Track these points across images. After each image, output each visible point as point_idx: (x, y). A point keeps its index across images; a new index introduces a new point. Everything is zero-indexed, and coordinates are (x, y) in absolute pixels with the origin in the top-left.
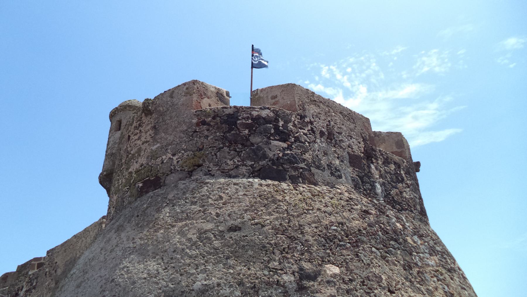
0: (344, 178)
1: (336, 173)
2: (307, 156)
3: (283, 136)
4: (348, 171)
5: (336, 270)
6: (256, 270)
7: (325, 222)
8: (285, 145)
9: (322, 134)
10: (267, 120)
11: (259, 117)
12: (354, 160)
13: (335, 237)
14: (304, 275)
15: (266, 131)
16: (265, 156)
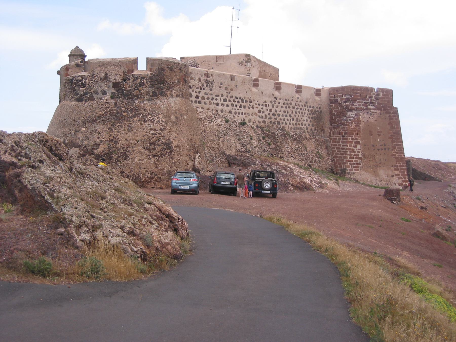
0: (108, 94)
1: (104, 93)
2: (92, 91)
3: (84, 85)
4: (112, 90)
7: (87, 115)
8: (84, 89)
9: (101, 79)
10: (80, 81)
11: (78, 80)
13: (88, 120)
14: (76, 131)
16: (78, 94)
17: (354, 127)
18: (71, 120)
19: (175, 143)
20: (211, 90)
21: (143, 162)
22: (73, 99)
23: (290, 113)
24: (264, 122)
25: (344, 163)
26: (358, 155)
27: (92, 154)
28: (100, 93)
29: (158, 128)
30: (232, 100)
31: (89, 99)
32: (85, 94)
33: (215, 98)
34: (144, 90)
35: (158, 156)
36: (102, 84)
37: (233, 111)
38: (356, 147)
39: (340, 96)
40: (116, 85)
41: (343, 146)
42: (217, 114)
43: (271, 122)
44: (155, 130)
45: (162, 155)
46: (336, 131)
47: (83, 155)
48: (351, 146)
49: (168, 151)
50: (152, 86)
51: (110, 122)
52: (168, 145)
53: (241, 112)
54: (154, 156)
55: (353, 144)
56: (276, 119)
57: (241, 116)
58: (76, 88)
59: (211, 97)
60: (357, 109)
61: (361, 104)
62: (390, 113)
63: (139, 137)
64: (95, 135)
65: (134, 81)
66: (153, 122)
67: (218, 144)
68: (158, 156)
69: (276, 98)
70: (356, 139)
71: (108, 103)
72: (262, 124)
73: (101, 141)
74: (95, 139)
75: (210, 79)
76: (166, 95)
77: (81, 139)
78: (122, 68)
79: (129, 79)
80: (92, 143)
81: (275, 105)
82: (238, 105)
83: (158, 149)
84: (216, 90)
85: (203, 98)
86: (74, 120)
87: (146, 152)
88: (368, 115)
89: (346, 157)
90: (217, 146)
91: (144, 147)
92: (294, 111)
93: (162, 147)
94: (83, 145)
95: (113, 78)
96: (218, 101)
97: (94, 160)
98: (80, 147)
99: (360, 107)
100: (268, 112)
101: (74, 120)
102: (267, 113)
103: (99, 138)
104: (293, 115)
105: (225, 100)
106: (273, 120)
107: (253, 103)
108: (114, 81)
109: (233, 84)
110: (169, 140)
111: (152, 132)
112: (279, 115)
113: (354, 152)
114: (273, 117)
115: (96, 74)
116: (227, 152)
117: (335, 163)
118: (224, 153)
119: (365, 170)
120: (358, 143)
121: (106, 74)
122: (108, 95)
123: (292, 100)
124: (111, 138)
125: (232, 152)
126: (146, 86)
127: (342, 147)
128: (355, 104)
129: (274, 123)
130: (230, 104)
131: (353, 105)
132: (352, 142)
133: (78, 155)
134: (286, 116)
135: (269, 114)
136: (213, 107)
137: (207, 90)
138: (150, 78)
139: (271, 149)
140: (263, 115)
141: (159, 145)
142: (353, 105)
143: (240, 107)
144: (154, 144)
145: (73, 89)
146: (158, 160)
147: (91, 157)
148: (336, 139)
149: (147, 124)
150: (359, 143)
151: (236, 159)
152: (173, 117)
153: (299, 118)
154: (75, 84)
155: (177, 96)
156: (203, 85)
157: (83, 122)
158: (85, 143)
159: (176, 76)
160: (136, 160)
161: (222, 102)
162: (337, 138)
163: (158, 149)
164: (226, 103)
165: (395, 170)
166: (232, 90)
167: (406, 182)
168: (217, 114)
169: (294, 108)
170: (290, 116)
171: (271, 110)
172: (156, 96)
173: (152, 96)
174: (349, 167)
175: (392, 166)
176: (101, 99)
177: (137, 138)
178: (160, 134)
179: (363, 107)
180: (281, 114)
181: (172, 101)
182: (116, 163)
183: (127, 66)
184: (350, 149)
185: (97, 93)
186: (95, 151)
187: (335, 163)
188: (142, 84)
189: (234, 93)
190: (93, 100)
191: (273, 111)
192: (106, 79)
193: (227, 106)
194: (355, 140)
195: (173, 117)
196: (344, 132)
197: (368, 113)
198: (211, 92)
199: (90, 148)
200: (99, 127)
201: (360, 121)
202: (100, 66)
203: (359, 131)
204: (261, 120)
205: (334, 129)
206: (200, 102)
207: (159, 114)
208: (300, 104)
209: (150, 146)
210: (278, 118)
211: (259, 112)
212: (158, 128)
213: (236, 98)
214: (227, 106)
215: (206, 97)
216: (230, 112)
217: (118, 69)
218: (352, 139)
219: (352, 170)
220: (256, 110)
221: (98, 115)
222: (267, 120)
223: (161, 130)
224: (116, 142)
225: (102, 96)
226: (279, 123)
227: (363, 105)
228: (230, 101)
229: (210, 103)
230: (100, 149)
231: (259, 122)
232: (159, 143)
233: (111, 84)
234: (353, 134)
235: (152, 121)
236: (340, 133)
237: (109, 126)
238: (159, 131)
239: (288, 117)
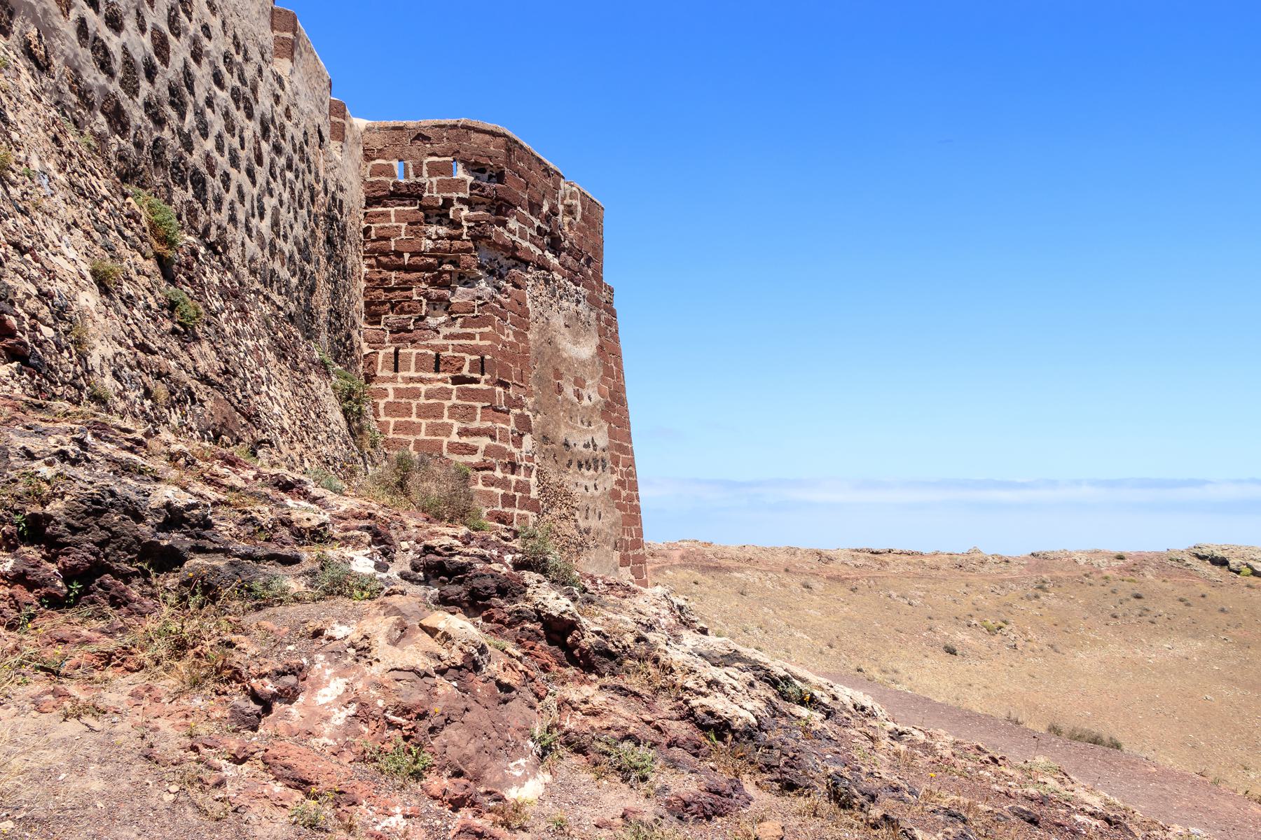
17: (511, 338)
26: (524, 487)
38: (518, 442)
39: (434, 170)
41: (463, 432)
46: (409, 351)
61: (529, 231)
70: (518, 403)
99: (526, 244)
113: (513, 467)
120: (524, 425)
123: (260, 71)
127: (455, 438)
128: (513, 224)
131: (504, 224)
134: (234, 162)
135: (151, 73)
139: (204, 379)
140: (114, 43)
142: (504, 224)
148: (416, 394)
153: (286, 216)
162: (423, 388)
170: (251, 173)
175: (615, 547)
179: (533, 248)
180: (217, 123)
191: (170, 73)
194: (515, 406)
196: (468, 358)
197: (547, 282)
201: (526, 313)
226: (199, 183)
227: (532, 240)
234: (506, 371)
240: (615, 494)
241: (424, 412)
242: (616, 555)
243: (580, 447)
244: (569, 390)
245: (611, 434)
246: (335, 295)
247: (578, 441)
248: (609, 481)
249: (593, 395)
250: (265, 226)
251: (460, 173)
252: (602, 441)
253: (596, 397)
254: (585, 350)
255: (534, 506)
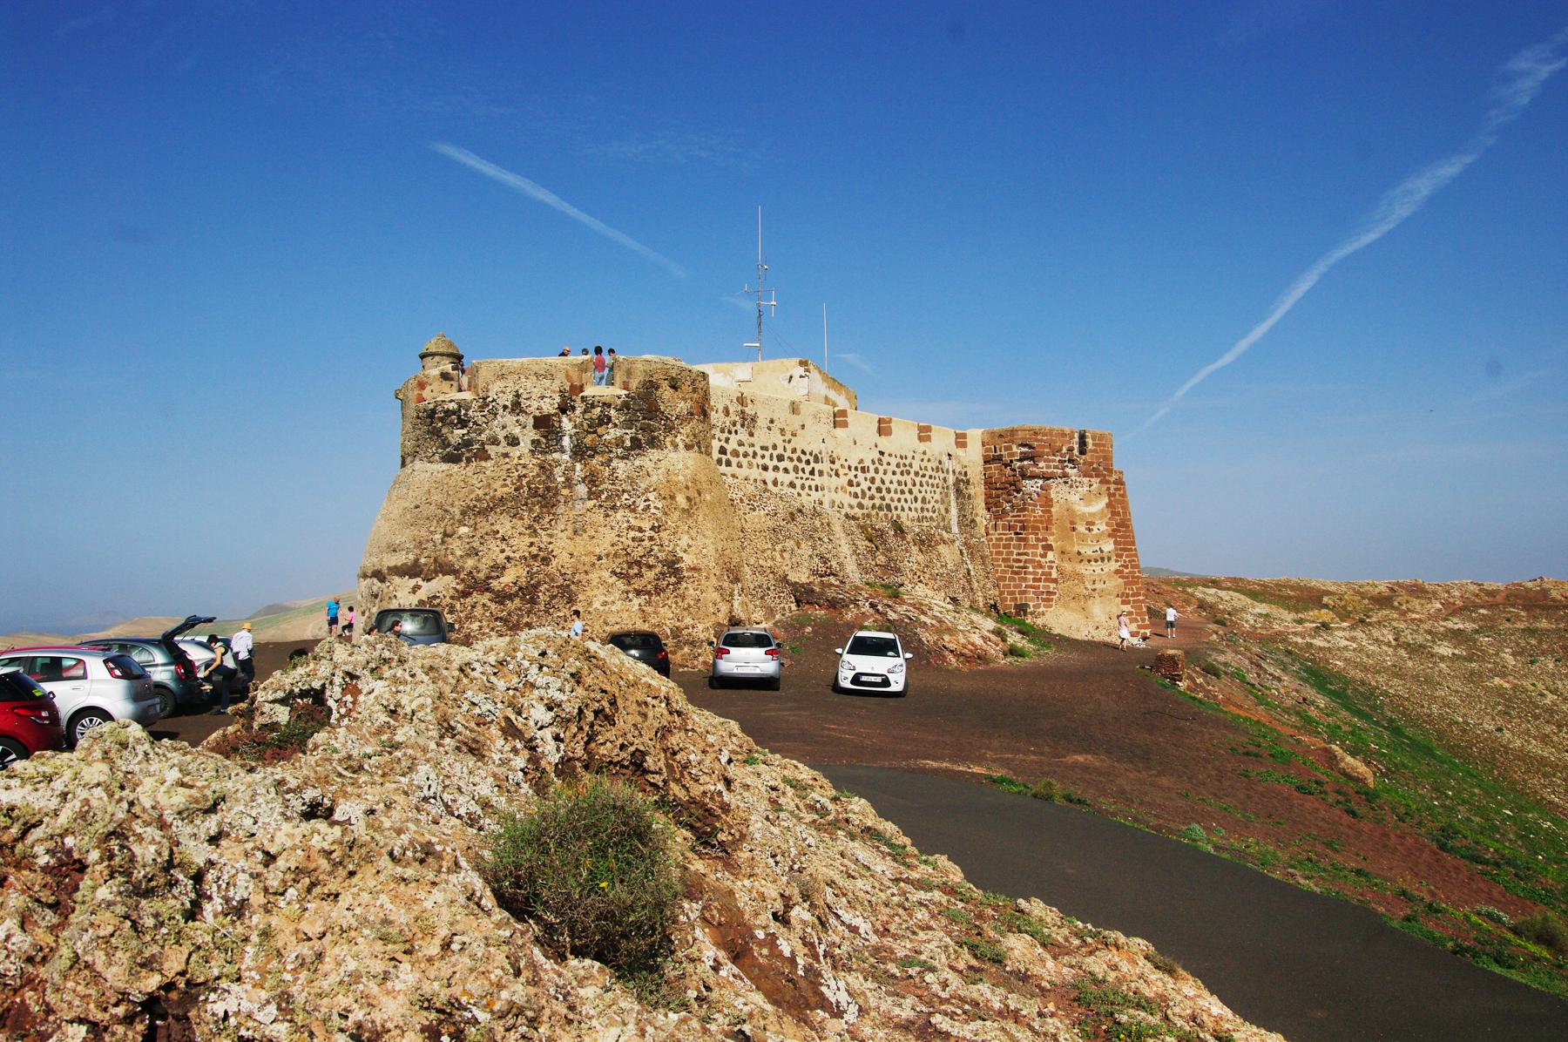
1: (513, 441)
3: (463, 423)
4: (532, 434)
5: (464, 530)
6: (424, 533)
8: (465, 431)
9: (505, 407)
10: (454, 412)
12: (542, 422)
14: (446, 535)
15: (452, 423)
16: (449, 445)
18: (433, 507)
19: (688, 560)
20: (751, 435)
21: (613, 608)
22: (437, 457)
23: (910, 485)
24: (860, 506)
25: (1022, 593)
27: (487, 590)
28: (504, 443)
29: (646, 525)
30: (795, 456)
31: (475, 456)
32: (467, 444)
33: (760, 452)
34: (612, 434)
35: (649, 593)
36: (510, 419)
37: (798, 483)
38: (1044, 556)
39: (1007, 448)
40: (542, 422)
42: (766, 490)
43: (873, 507)
44: (640, 530)
45: (658, 590)
47: (465, 594)
48: (1034, 554)
49: (673, 580)
50: (629, 424)
51: (531, 510)
52: (672, 566)
53: (813, 484)
54: (638, 593)
55: (1040, 551)
56: (883, 498)
57: (813, 492)
58: (444, 431)
59: (750, 451)
60: (1046, 478)
62: (1108, 482)
63: (603, 547)
64: (494, 545)
65: (585, 412)
66: (634, 511)
67: (773, 559)
68: (649, 593)
69: (882, 453)
70: (1045, 540)
71: (524, 466)
72: (856, 510)
73: (508, 559)
74: (495, 551)
75: (749, 410)
76: (661, 447)
77: (459, 553)
78: (557, 382)
79: (573, 408)
80: (485, 564)
81: (881, 469)
82: (808, 469)
83: (650, 575)
84: (761, 437)
85: (736, 454)
86: (440, 507)
87: (621, 585)
88: (1066, 488)
89: (1025, 580)
90: (770, 563)
91: (614, 573)
92: (917, 480)
93: (657, 570)
94: (462, 568)
95: (535, 405)
96: (767, 461)
97: (493, 606)
98: (456, 573)
100: (868, 484)
101: (440, 507)
102: (865, 485)
103: (503, 551)
104: (915, 490)
105: (781, 458)
106: (877, 502)
107: (837, 466)
108: (537, 413)
109: (796, 421)
110: (673, 553)
111: (632, 534)
112: (889, 491)
113: (1041, 567)
114: (878, 495)
115: (492, 395)
116: (793, 577)
117: (1001, 593)
118: (784, 579)
119: (1065, 606)
120: (1049, 548)
121: (518, 396)
122: (525, 446)
124: (534, 550)
125: (801, 576)
126: (615, 425)
129: (880, 508)
130: (790, 466)
132: (1035, 547)
133: (452, 592)
134: (902, 492)
136: (755, 473)
137: (743, 435)
138: (626, 405)
140: (858, 490)
141: (650, 567)
143: (812, 473)
144: (638, 563)
145: (436, 433)
146: (649, 603)
147: (485, 598)
149: (621, 513)
150: (1050, 548)
151: (813, 591)
152: (681, 500)
153: (928, 496)
154: (441, 419)
155: (688, 447)
156: (734, 424)
157: (463, 513)
158: (470, 563)
159: (684, 399)
160: (597, 604)
161: (775, 462)
163: (650, 575)
164: (782, 465)
165: (1124, 603)
166: (794, 435)
167: (1146, 627)
168: (766, 490)
169: (917, 474)
170: (911, 492)
171: (873, 480)
172: (640, 447)
173: (632, 448)
174: (1032, 600)
176: (506, 455)
177: (597, 551)
178: (651, 539)
180: (893, 487)
181: (674, 461)
182: (547, 612)
183: (568, 376)
184: (1033, 561)
185: (495, 441)
186: (494, 584)
187: (1001, 593)
188: (604, 420)
189: (799, 443)
190: (488, 458)
192: (516, 407)
193: (786, 470)
195: (681, 500)
198: (751, 440)
199: (481, 575)
200: (504, 525)
202: (502, 377)
203: (1049, 521)
204: (855, 502)
205: (996, 518)
206: (729, 464)
207: (647, 490)
208: (929, 465)
209: (629, 569)
210: (888, 497)
211: (850, 484)
212: (646, 525)
213: (804, 452)
214: (786, 470)
215: (741, 450)
216: (792, 485)
217: (547, 383)
218: (1038, 540)
219: (1037, 606)
220: (843, 480)
221: (498, 494)
222: (866, 502)
223: (653, 528)
224: (546, 561)
225: (509, 449)
226: (888, 506)
228: (791, 459)
229: (750, 465)
230: (508, 578)
231: (851, 507)
232: (651, 561)
233: (531, 421)
235: (632, 508)
236: (1010, 528)
237: (527, 522)
238: (649, 533)
239: (907, 496)
240: (1117, 572)
241: (1005, 547)
242: (1119, 600)
243: (1089, 552)
244: (1081, 529)
245: (1116, 543)
246: (961, 509)
247: (1088, 551)
248: (1114, 566)
249: (1101, 527)
250: (919, 505)
251: (1015, 449)
252: (1108, 546)
253: (1104, 528)
254: (1100, 504)
255: (1055, 581)
